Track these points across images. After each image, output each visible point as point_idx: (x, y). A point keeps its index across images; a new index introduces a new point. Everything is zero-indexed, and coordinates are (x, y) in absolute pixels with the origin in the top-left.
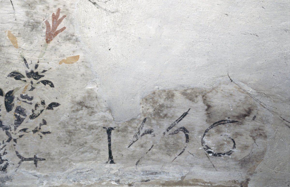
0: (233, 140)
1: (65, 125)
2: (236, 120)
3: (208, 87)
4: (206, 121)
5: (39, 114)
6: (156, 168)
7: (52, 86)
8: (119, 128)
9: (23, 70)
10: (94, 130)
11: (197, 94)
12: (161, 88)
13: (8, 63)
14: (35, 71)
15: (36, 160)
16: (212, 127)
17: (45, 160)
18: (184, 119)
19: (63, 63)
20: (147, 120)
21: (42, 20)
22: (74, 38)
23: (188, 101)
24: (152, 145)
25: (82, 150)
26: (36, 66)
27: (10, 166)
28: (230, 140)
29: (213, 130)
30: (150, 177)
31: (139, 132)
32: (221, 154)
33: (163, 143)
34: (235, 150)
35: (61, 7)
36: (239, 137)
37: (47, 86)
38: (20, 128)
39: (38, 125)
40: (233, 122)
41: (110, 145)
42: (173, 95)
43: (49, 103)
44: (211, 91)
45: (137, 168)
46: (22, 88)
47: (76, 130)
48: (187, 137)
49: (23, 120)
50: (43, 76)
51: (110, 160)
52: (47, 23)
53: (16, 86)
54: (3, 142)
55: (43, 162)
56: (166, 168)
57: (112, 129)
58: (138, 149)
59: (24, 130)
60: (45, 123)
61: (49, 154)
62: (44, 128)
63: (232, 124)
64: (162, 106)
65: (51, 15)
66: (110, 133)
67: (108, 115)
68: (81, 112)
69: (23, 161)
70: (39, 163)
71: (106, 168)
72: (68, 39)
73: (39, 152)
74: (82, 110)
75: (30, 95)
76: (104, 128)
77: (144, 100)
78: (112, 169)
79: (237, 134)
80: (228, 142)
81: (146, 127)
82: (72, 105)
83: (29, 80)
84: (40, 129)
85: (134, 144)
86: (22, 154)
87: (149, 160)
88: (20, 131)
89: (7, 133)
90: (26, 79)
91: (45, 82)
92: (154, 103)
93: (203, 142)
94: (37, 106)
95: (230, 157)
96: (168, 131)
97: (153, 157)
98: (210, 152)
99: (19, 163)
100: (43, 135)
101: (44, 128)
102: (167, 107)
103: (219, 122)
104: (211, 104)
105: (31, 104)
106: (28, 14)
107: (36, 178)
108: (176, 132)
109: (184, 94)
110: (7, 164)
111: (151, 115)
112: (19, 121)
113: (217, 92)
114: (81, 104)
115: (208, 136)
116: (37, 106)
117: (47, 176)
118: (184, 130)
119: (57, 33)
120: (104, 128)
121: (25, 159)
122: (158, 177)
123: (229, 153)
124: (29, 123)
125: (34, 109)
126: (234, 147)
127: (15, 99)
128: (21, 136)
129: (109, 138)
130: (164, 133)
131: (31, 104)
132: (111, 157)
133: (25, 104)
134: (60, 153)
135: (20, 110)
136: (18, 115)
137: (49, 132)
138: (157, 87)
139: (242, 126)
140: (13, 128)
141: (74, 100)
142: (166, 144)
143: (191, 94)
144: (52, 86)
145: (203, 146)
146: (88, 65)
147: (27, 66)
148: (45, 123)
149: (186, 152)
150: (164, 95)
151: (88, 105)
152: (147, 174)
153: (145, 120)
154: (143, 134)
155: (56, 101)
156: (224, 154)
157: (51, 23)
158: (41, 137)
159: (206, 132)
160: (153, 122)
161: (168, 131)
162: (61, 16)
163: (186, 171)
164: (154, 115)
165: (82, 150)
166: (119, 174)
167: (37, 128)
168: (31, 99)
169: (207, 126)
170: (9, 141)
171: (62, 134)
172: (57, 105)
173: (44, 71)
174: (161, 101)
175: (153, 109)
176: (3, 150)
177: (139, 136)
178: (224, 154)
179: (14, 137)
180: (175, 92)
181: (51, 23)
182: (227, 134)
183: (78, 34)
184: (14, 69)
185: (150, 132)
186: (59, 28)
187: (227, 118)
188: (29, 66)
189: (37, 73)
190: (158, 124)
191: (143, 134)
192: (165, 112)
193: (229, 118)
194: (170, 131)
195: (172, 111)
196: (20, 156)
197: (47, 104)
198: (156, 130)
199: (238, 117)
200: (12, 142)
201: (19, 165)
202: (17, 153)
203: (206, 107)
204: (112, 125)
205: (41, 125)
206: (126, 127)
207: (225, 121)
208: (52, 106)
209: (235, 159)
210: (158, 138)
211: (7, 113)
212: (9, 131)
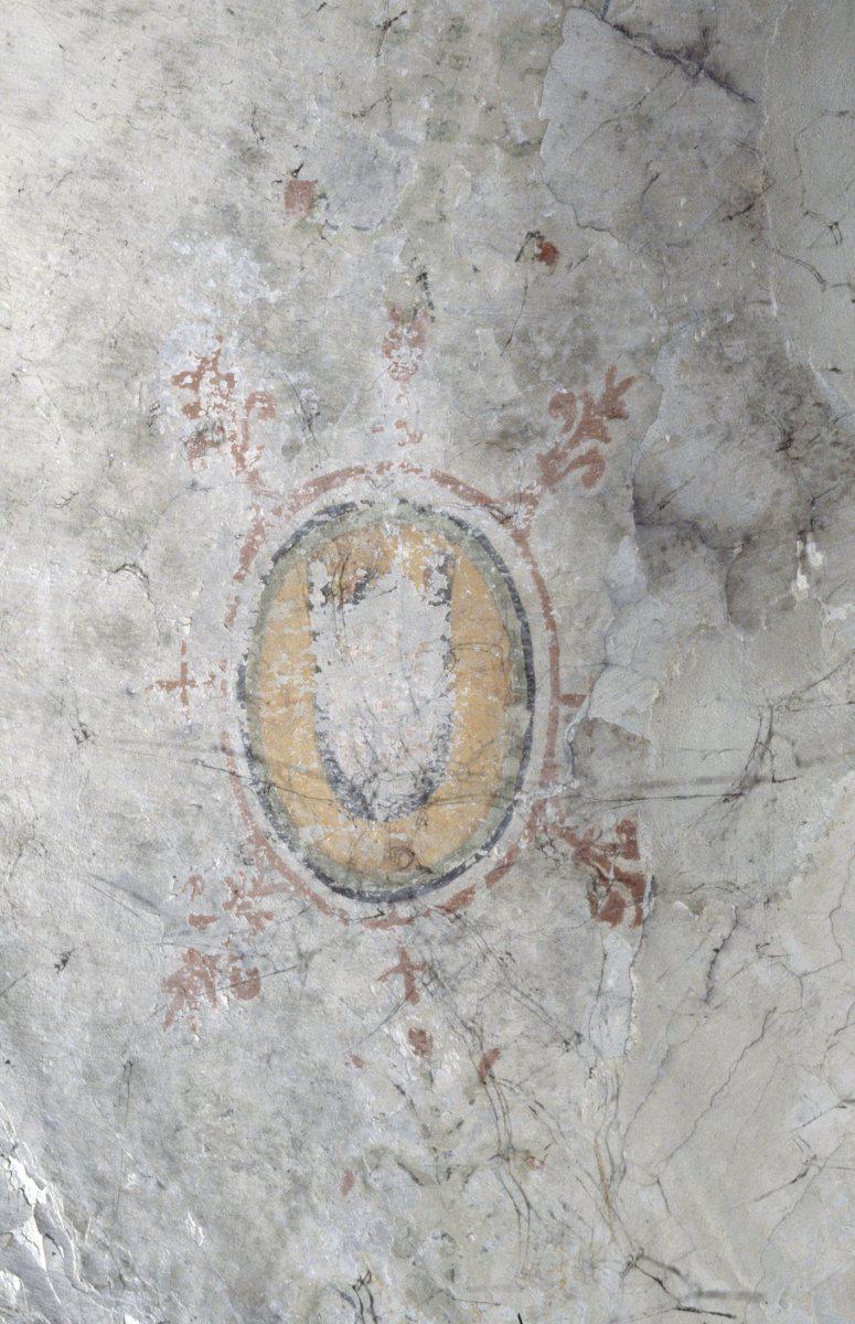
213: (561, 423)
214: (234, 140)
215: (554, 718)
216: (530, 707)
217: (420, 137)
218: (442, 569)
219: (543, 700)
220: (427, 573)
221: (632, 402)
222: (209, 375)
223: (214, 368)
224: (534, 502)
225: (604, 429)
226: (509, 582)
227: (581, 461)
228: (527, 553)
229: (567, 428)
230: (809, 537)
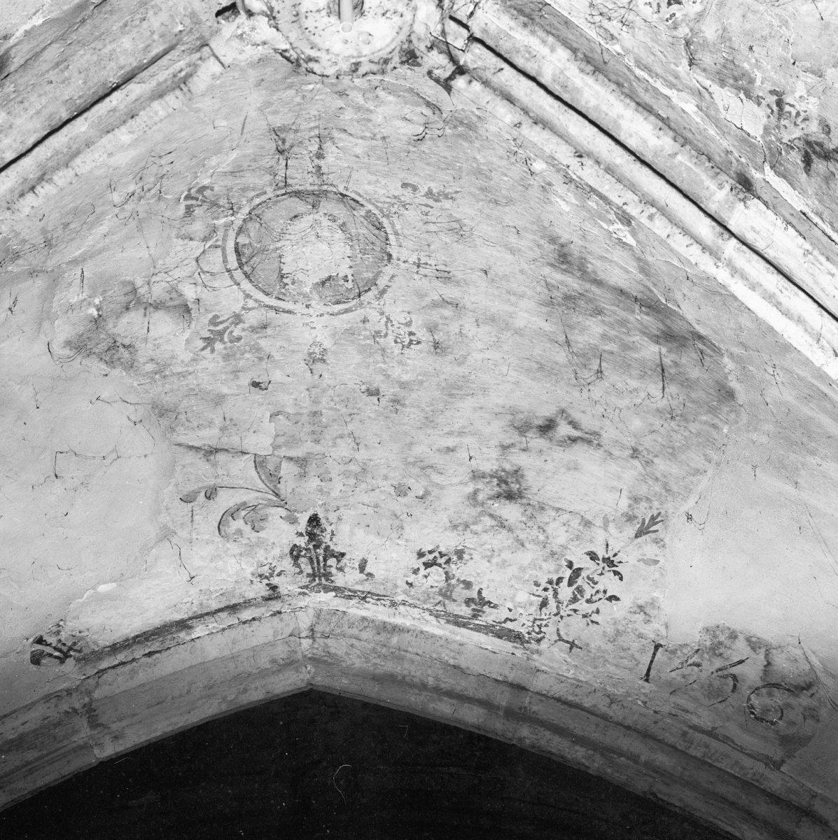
3: (774, 643)
7: (621, 579)
9: (601, 553)
12: (727, 625)
13: (591, 541)
16: (764, 687)
18: (739, 666)
21: (640, 516)
22: (662, 543)
23: (749, 648)
25: (622, 654)
26: (615, 555)
27: (546, 640)
29: (764, 691)
31: (687, 661)
33: (708, 682)
34: (780, 722)
35: (663, 512)
36: (789, 709)
40: (788, 690)
41: (652, 662)
46: (592, 570)
48: (735, 686)
49: (578, 600)
52: (644, 520)
53: (587, 566)
57: (661, 646)
59: (575, 611)
61: (588, 645)
62: (595, 617)
64: (720, 643)
65: (650, 515)
67: (663, 632)
68: (637, 616)
69: (559, 640)
70: (574, 649)
72: (656, 541)
75: (596, 579)
80: (776, 711)
81: (696, 659)
83: (602, 565)
86: (562, 633)
89: (558, 607)
90: (600, 562)
91: (616, 573)
93: (749, 699)
94: (598, 592)
98: (753, 713)
99: (556, 641)
100: (590, 623)
102: (725, 647)
104: (773, 662)
105: (593, 588)
106: (630, 506)
108: (725, 677)
109: (748, 640)
110: (544, 637)
112: (574, 600)
113: (783, 652)
114: (640, 607)
115: (758, 695)
116: (598, 592)
117: (576, 666)
118: (734, 677)
119: (648, 532)
121: (563, 640)
122: (688, 716)
124: (582, 606)
126: (781, 718)
127: (581, 577)
128: (569, 615)
129: (654, 654)
131: (593, 588)
135: (580, 590)
137: (597, 623)
140: (565, 604)
143: (754, 643)
144: (621, 579)
147: (607, 551)
148: (598, 612)
150: (727, 633)
151: (648, 612)
152: (679, 709)
154: (690, 665)
155: (618, 596)
157: (647, 522)
159: (756, 689)
160: (705, 655)
162: (659, 519)
168: (596, 583)
169: (760, 684)
170: (555, 615)
172: (617, 599)
173: (620, 562)
174: (722, 638)
177: (685, 665)
179: (562, 613)
181: (647, 522)
183: (667, 541)
184: (594, 549)
185: (698, 665)
186: (652, 529)
187: (783, 684)
189: (613, 561)
192: (721, 651)
196: (559, 635)
197: (608, 594)
199: (796, 687)
200: (558, 618)
202: (558, 630)
203: (766, 663)
204: (662, 642)
205: (593, 612)
206: (676, 650)
208: (613, 598)
209: (777, 732)
213: (235, 334)
214: (404, 405)
215: (224, 240)
216: (237, 244)
217: (324, 411)
218: (287, 284)
219: (230, 245)
220: (293, 283)
221: (201, 344)
222: (406, 343)
223: (403, 346)
224: (243, 308)
225: (212, 333)
226: (251, 281)
227: (221, 323)
228: (244, 292)
229: (232, 332)
230: (96, 316)
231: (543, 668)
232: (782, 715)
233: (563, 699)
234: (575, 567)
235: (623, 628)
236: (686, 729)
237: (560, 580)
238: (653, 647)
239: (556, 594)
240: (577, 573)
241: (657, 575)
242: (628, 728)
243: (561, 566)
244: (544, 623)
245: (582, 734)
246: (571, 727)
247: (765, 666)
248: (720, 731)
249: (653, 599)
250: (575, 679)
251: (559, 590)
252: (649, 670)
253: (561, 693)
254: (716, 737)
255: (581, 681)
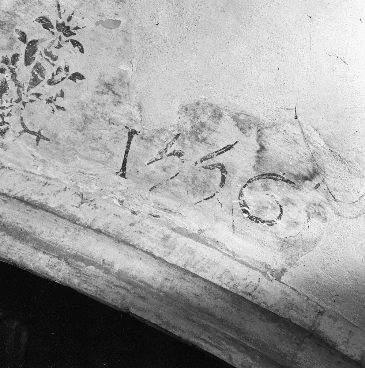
0: (280, 206)
1: (83, 106)
2: (292, 180)
3: (268, 121)
4: (254, 167)
5: (59, 82)
6: (172, 204)
7: (82, 51)
8: (144, 134)
9: (54, 19)
10: (114, 126)
11: (252, 125)
14: (67, 24)
15: (39, 136)
16: (258, 178)
17: (49, 140)
19: (100, 25)
20: (180, 137)
23: (237, 129)
24: (177, 173)
25: (93, 145)
26: (70, 19)
27: (10, 132)
28: (277, 206)
29: (258, 183)
30: (161, 213)
31: (166, 150)
32: (259, 219)
33: (191, 175)
34: (278, 221)
36: (290, 205)
37: (77, 48)
38: (33, 91)
39: (54, 95)
40: (287, 181)
41: (127, 153)
42: (220, 116)
43: (73, 72)
44: (270, 128)
45: (149, 195)
46: (48, 42)
47: (94, 119)
48: (223, 179)
50: (75, 34)
51: (122, 172)
53: (42, 36)
54: (12, 100)
55: (46, 142)
56: (184, 210)
57: (136, 132)
58: (159, 172)
59: (38, 95)
60: (62, 95)
61: (55, 135)
62: (60, 102)
63: (285, 183)
64: (203, 125)
66: (132, 137)
68: (105, 96)
69: (25, 131)
70: (41, 141)
71: (113, 180)
73: (45, 127)
74: (108, 94)
75: (54, 54)
76: (126, 127)
77: (184, 109)
78: (120, 184)
79: (288, 201)
80: (274, 208)
81: (176, 147)
82: (98, 84)
84: (55, 100)
85: (156, 163)
86: (26, 123)
87: (167, 190)
88: (33, 94)
89: (18, 92)
90: (55, 31)
91: (75, 43)
92: (194, 117)
93: (241, 195)
95: (270, 228)
96: (201, 161)
97: (173, 189)
98: (245, 212)
99: (21, 133)
101: (60, 102)
103: (269, 174)
104: (266, 146)
107: (33, 158)
108: (211, 168)
109: (235, 118)
110: (8, 129)
111: (187, 132)
112: (35, 82)
115: (251, 188)
116: (59, 70)
117: (45, 161)
118: (223, 168)
120: (126, 127)
121: (28, 131)
123: (271, 223)
124: (44, 88)
125: (55, 73)
127: (38, 52)
128: (31, 101)
129: (129, 143)
130: (196, 163)
131: (53, 65)
132: (124, 168)
133: (47, 63)
134: (68, 139)
135: (39, 69)
136: (36, 73)
138: (204, 97)
139: (300, 193)
140: (26, 88)
141: (102, 78)
142: (195, 179)
143: (243, 122)
144: (82, 51)
145: (240, 199)
146: (128, 38)
147: (60, 14)
148: (62, 95)
149: (215, 199)
151: (116, 91)
153: (177, 136)
154: (170, 155)
155: (82, 73)
156: (263, 222)
158: (53, 110)
159: (249, 182)
160: (187, 142)
161: (201, 161)
163: (207, 224)
164: (191, 133)
165: (93, 145)
166: (126, 194)
167: (52, 98)
168: (55, 59)
169: (253, 174)
170: (17, 101)
171: (78, 117)
172: (82, 77)
173: (77, 28)
174: (204, 118)
175: (191, 125)
176: (9, 110)
177: (165, 155)
178: (263, 222)
179: (24, 99)
180: (224, 112)
182: (275, 195)
184: (45, 14)
185: (179, 155)
187: (281, 173)
188: (62, 15)
189: (68, 27)
190: (192, 147)
191: (170, 155)
192: (205, 135)
193: (284, 174)
194: (205, 163)
195: (214, 135)
196: (23, 125)
197: (71, 72)
198: (187, 153)
199: (297, 177)
200: (20, 105)
201: (19, 135)
202: (22, 119)
203: (258, 148)
205: (57, 95)
206: (153, 137)
207: (278, 176)
208: (77, 76)
209: (276, 235)
210: (187, 166)
211: (25, 67)
212: (21, 89)
231: (10, 164)
232: (281, 214)
233: (26, 198)
234: (29, 40)
235: (92, 114)
236: (168, 232)
237: (15, 57)
238: (127, 135)
239: (14, 76)
240: (32, 46)
241: (121, 42)
242: (99, 231)
243: (12, 39)
244: (6, 111)
245: (49, 239)
246: (38, 230)
247: (258, 152)
248: (208, 234)
249: (120, 74)
250: (43, 176)
251: (17, 70)
252: (125, 163)
253: (25, 193)
254: (204, 242)
255: (51, 179)
